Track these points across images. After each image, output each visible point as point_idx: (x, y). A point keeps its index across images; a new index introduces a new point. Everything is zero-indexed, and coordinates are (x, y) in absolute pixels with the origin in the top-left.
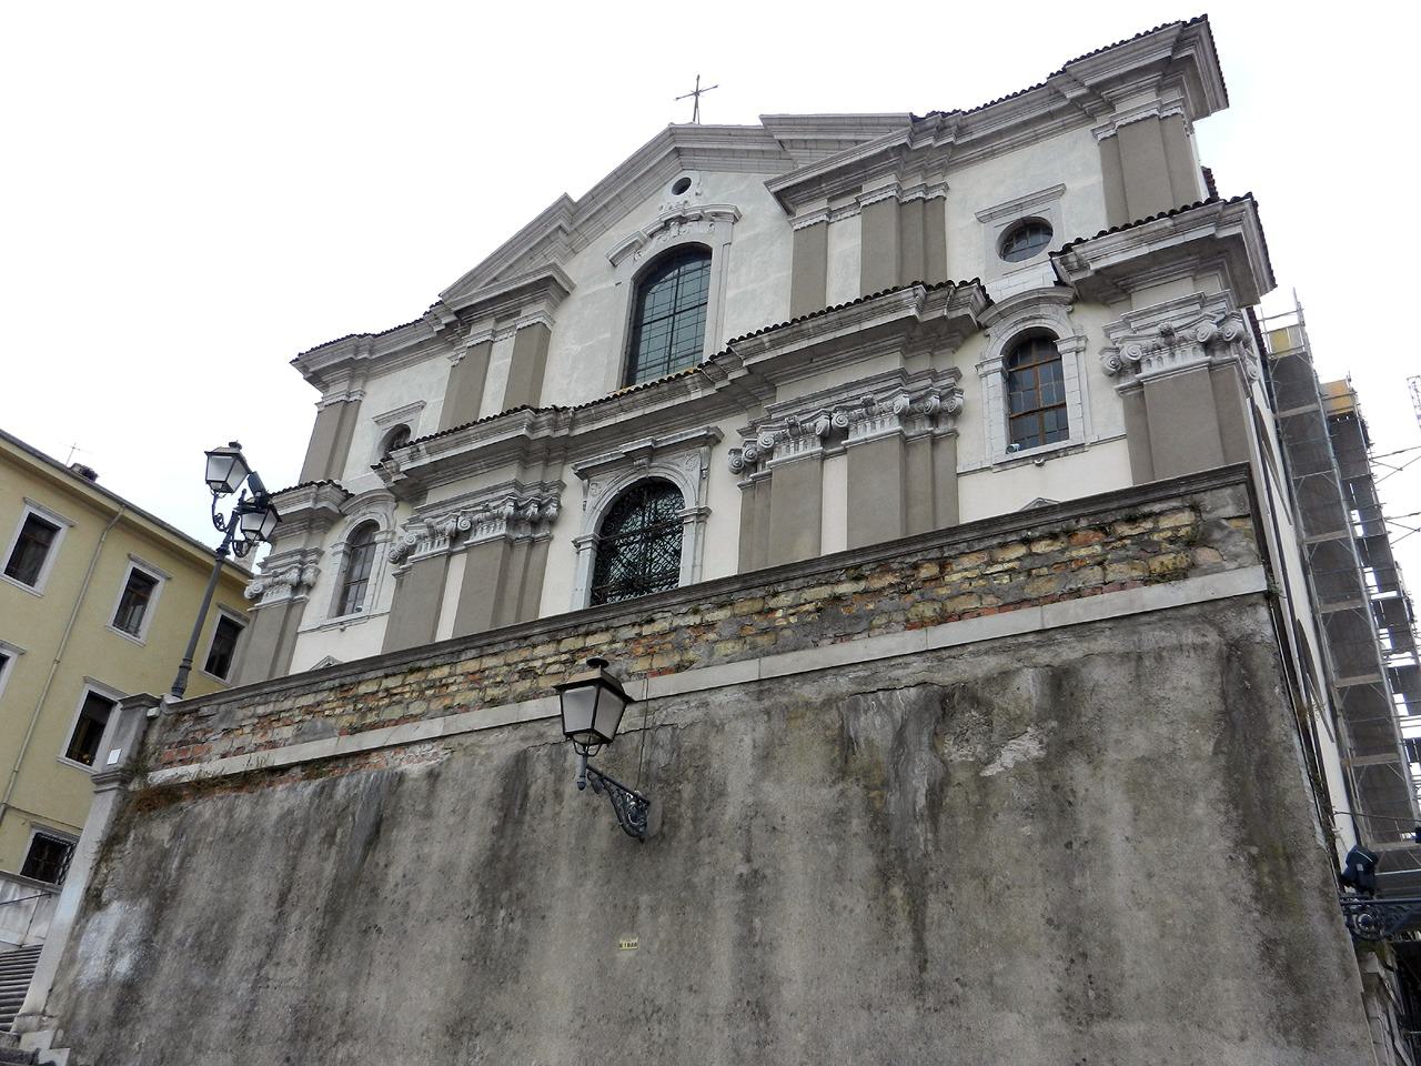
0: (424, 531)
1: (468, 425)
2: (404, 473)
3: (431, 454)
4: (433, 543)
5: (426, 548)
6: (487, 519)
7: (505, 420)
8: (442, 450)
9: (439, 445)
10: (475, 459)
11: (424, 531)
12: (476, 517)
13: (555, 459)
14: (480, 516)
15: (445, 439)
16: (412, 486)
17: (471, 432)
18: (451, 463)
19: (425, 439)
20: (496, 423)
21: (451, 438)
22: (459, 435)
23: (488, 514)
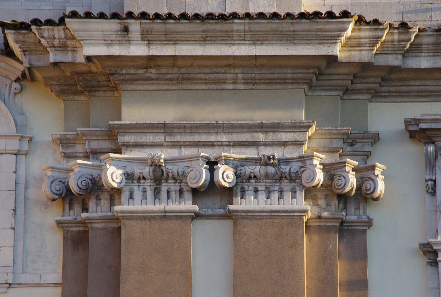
0: (147, 171)
1: (234, 16)
2: (89, 59)
3: (150, 42)
4: (157, 193)
5: (145, 198)
6: (267, 176)
7: (305, 25)
8: (175, 42)
9: (166, 33)
10: (228, 66)
11: (147, 171)
12: (248, 170)
13: (359, 92)
14: (257, 169)
15: (184, 26)
16: (78, 73)
17: (235, 27)
18: (180, 62)
19: (144, 15)
20: (286, 26)
21: (196, 26)
22: (212, 26)
23: (271, 170)
